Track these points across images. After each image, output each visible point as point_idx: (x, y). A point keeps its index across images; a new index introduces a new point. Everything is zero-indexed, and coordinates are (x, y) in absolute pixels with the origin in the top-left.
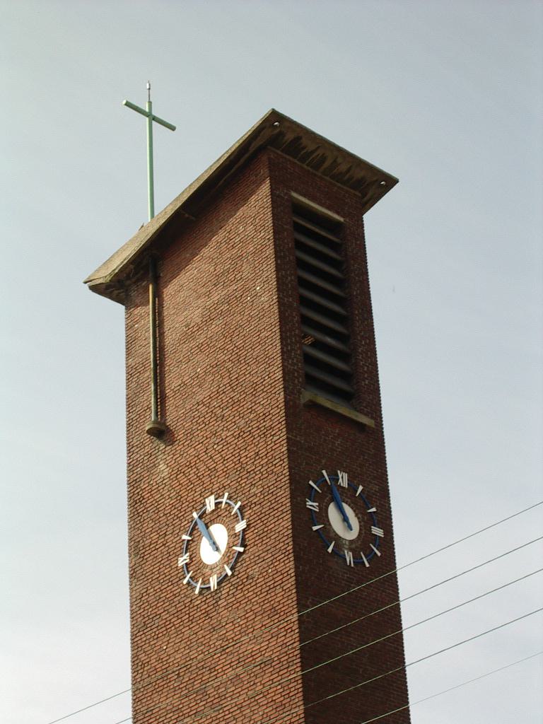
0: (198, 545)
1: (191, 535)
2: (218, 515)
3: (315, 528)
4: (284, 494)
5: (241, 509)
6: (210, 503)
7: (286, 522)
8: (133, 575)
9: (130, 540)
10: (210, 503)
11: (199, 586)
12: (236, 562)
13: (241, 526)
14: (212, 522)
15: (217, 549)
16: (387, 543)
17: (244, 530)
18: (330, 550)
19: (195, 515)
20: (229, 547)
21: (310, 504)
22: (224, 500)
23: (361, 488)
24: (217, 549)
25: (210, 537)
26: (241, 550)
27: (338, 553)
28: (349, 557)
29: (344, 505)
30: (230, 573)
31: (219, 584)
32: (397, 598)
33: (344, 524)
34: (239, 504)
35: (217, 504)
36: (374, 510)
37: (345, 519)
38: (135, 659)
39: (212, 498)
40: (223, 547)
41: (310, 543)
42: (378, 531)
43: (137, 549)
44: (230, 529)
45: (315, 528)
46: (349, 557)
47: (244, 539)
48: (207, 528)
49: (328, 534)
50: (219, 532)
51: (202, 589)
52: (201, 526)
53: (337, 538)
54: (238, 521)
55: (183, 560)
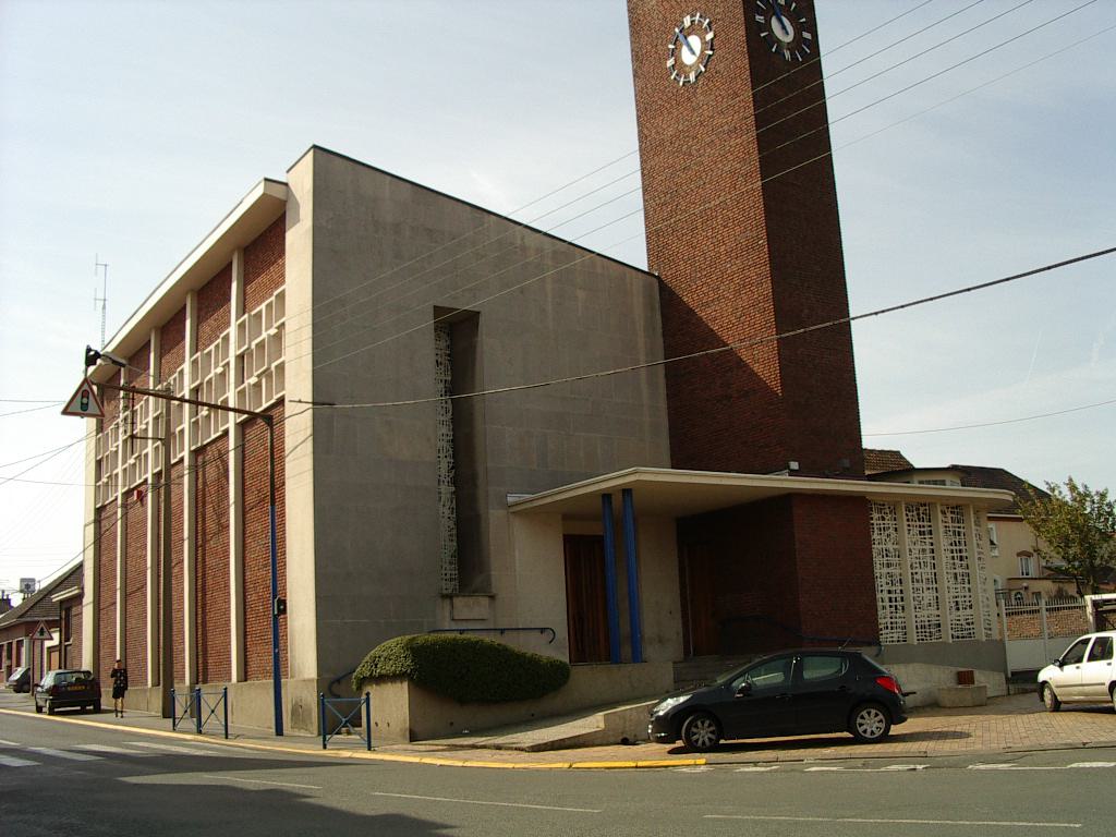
0: (680, 51)
1: (675, 44)
2: (693, 29)
3: (762, 35)
4: (739, 12)
5: (709, 24)
6: (687, 21)
7: (742, 32)
8: (636, 75)
9: (632, 51)
10: (687, 21)
11: (682, 79)
12: (708, 62)
13: (710, 36)
14: (689, 34)
15: (694, 53)
16: (814, 44)
17: (712, 39)
18: (773, 50)
19: (677, 30)
20: (702, 52)
21: (760, 18)
22: (697, 18)
23: (794, 5)
24: (694, 53)
25: (688, 45)
26: (711, 53)
27: (779, 52)
28: (787, 54)
29: (784, 19)
30: (703, 70)
31: (696, 77)
32: (822, 78)
33: (783, 31)
34: (708, 20)
35: (692, 22)
36: (804, 20)
37: (784, 28)
38: (640, 132)
39: (688, 17)
40: (698, 52)
41: (759, 47)
42: (807, 35)
43: (637, 57)
44: (702, 39)
45: (762, 35)
46: (787, 54)
47: (712, 46)
48: (686, 38)
49: (772, 38)
50: (694, 41)
51: (684, 82)
52: (681, 38)
53: (779, 41)
54: (707, 33)
55: (670, 62)
